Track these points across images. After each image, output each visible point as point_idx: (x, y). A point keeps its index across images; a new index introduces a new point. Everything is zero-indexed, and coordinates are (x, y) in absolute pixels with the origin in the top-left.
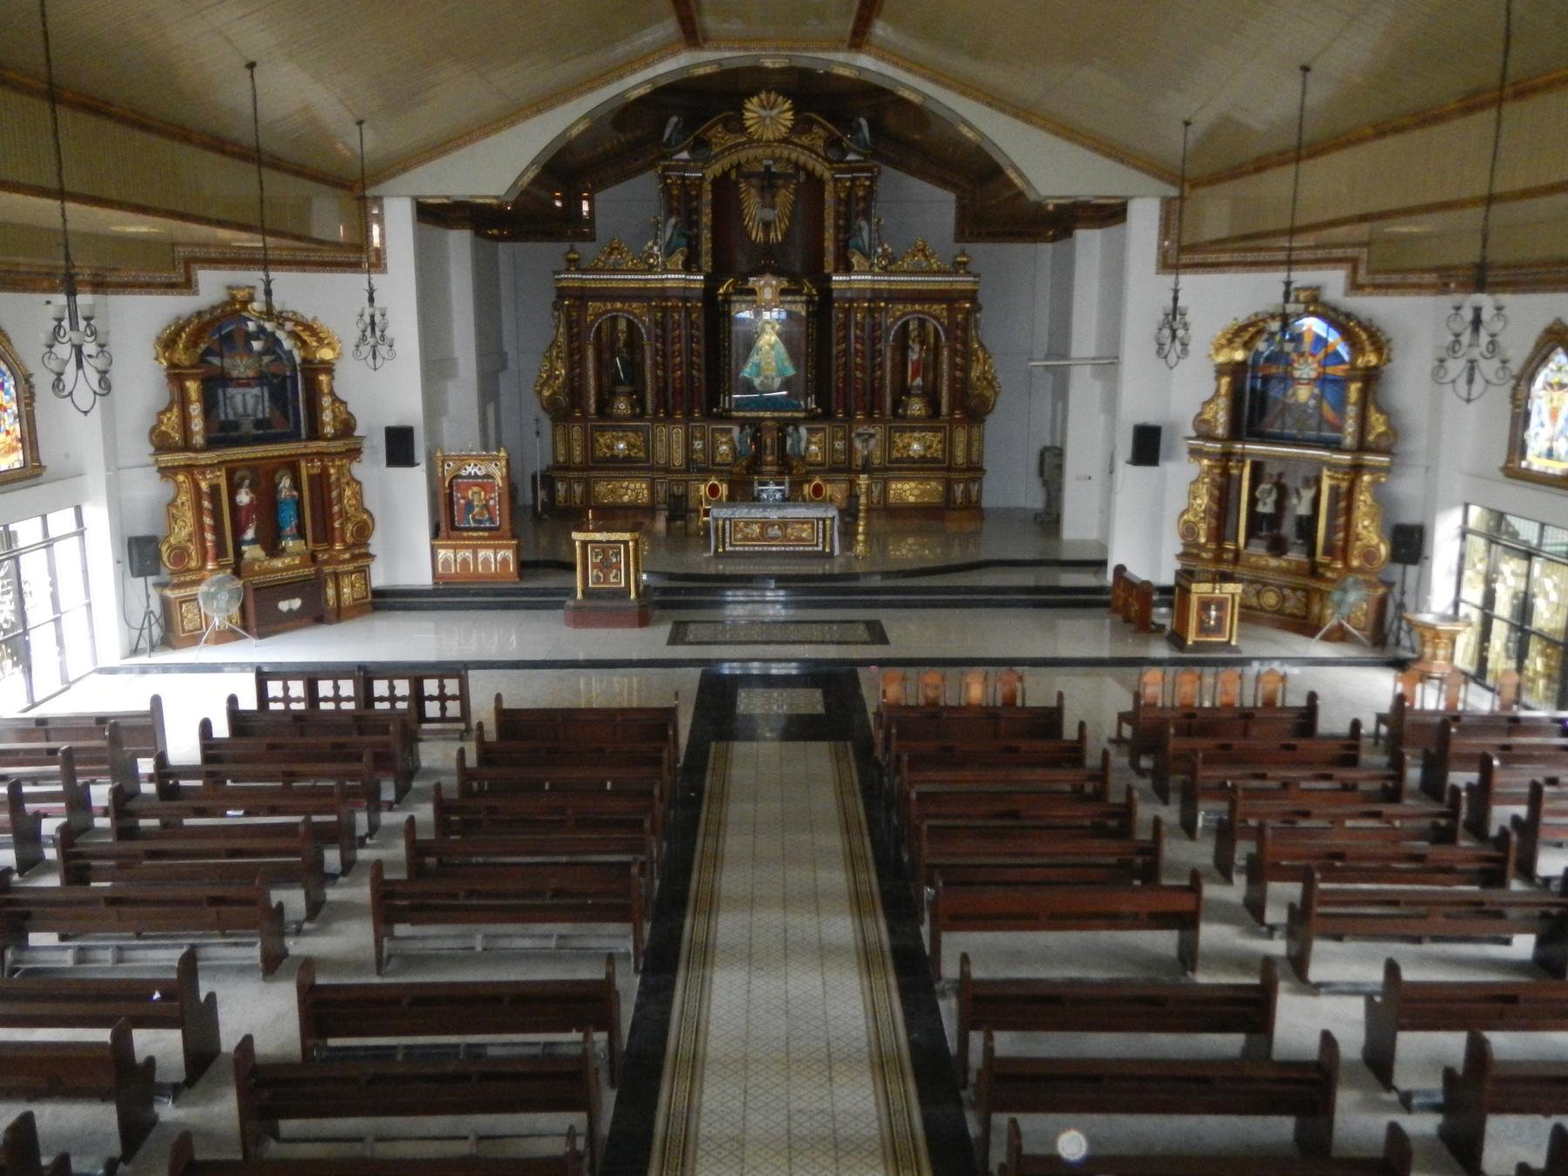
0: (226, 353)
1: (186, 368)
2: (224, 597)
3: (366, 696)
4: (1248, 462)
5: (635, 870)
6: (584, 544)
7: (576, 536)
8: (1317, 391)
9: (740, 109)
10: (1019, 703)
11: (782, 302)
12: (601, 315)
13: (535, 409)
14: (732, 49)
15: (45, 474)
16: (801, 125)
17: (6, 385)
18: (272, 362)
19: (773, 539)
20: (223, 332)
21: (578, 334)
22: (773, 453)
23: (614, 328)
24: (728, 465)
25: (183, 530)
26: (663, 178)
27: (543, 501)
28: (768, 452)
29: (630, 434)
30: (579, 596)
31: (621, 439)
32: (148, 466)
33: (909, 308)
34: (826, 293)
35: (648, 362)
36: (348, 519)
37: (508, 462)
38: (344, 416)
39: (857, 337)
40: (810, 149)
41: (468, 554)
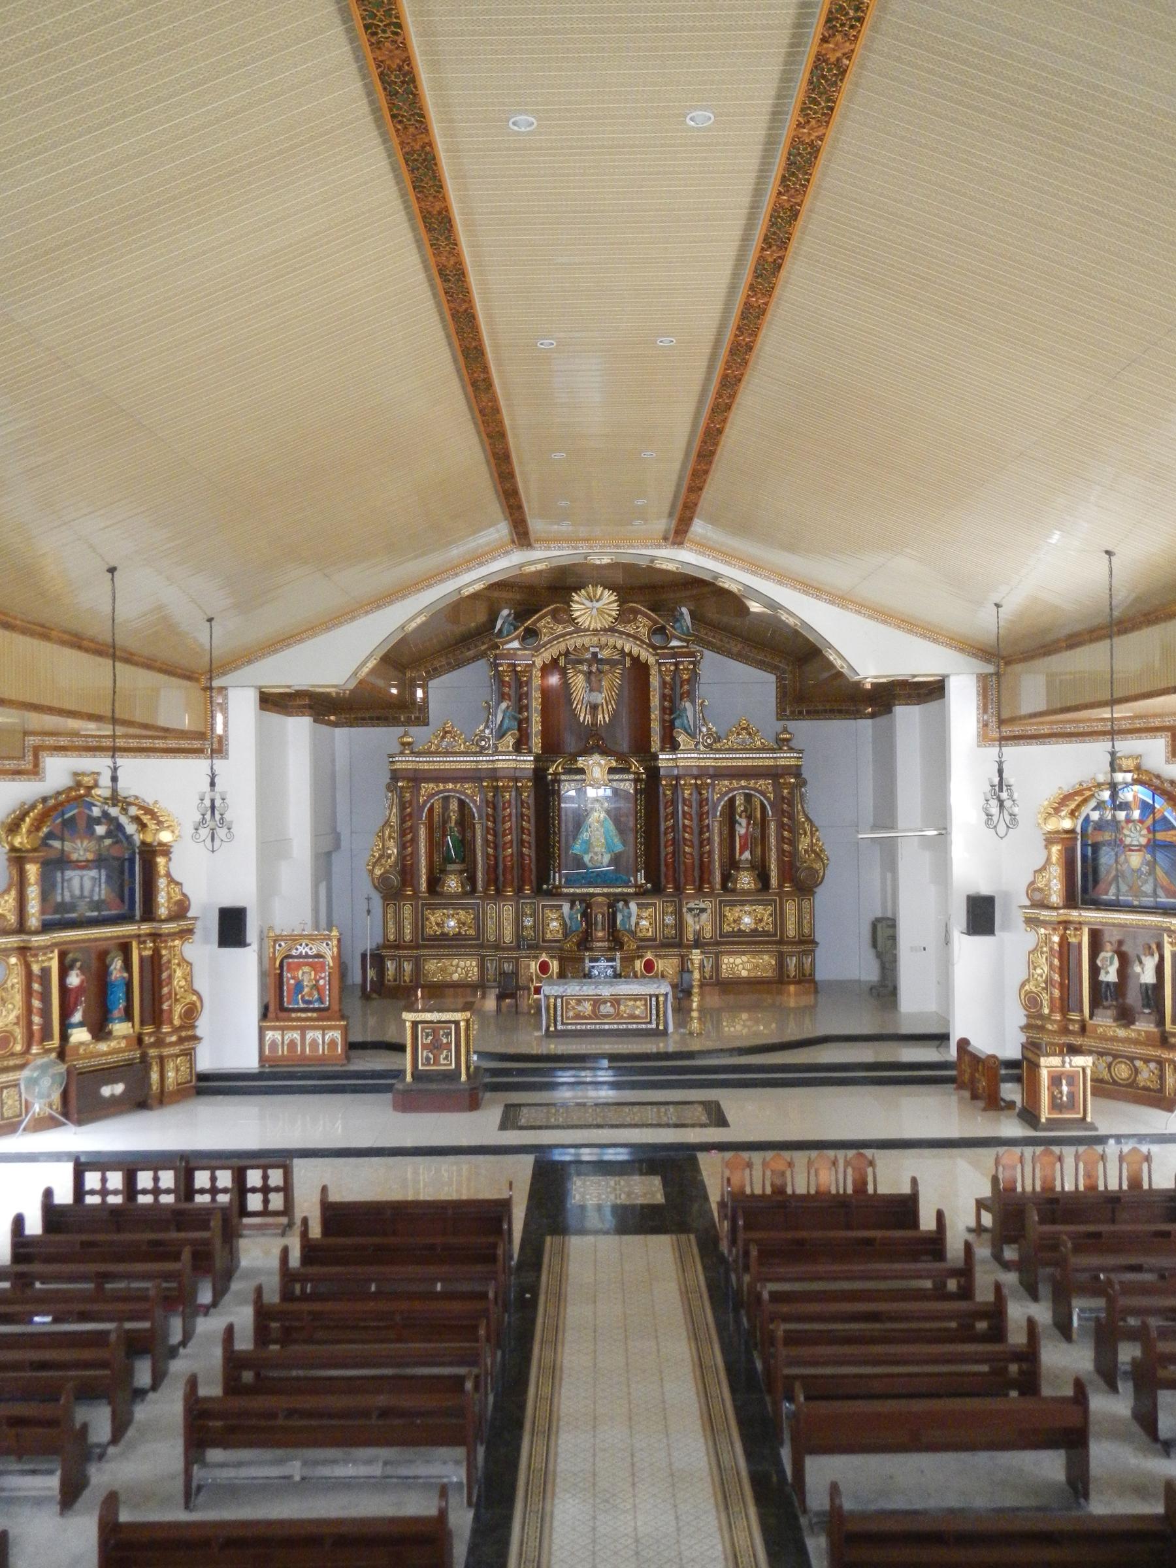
0: (67, 835)
1: (28, 851)
2: (46, 1082)
3: (186, 1189)
4: (1086, 931)
5: (469, 1385)
6: (415, 1024)
7: (409, 1016)
8: (1148, 857)
9: (568, 601)
10: (870, 1190)
11: (610, 781)
12: (433, 795)
13: (366, 887)
14: (560, 548)
16: (625, 615)
19: (605, 1016)
20: (66, 816)
21: (410, 815)
22: (603, 929)
23: (445, 808)
24: (556, 941)
26: (495, 666)
27: (372, 979)
28: (600, 927)
30: (409, 1078)
34: (653, 773)
35: (479, 841)
36: (177, 1000)
37: (339, 941)
38: (179, 897)
39: (684, 812)
40: (636, 638)
41: (296, 1035)
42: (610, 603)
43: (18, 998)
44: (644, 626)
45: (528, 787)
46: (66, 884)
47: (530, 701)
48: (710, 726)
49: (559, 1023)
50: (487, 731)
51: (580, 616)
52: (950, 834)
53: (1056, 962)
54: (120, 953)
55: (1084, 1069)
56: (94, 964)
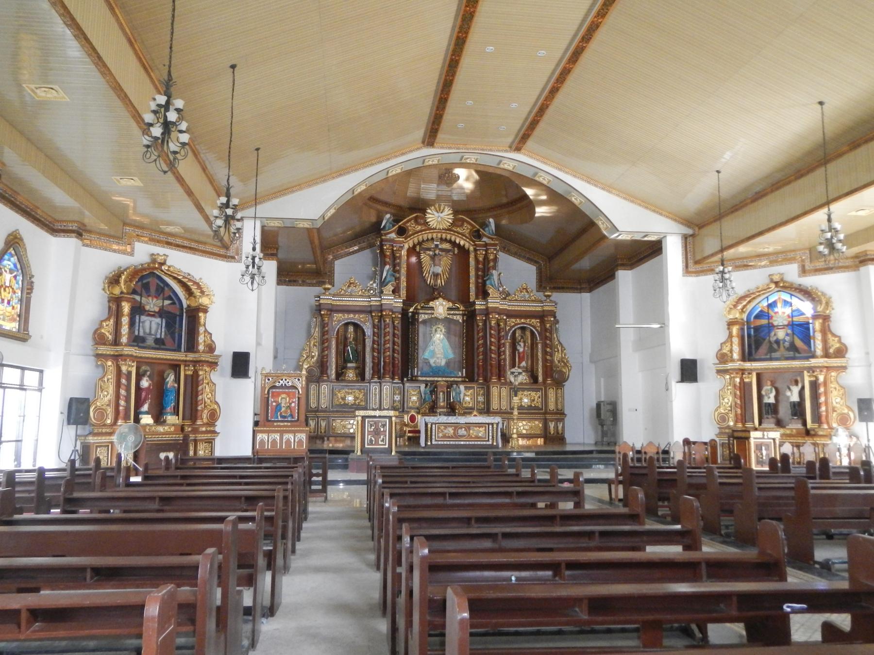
6: (364, 418)
8: (789, 331)
9: (424, 211)
14: (450, 148)
17: (18, 277)
18: (169, 304)
21: (327, 331)
25: (106, 397)
28: (441, 400)
29: (357, 391)
30: (359, 453)
32: (90, 355)
33: (518, 321)
41: (277, 436)
42: (448, 215)
43: (111, 389)
44: (468, 228)
45: (399, 318)
46: (141, 324)
47: (400, 268)
48: (505, 287)
49: (433, 440)
50: (375, 285)
51: (430, 221)
52: (668, 326)
53: (738, 393)
54: (173, 371)
55: (774, 439)
56: (156, 378)
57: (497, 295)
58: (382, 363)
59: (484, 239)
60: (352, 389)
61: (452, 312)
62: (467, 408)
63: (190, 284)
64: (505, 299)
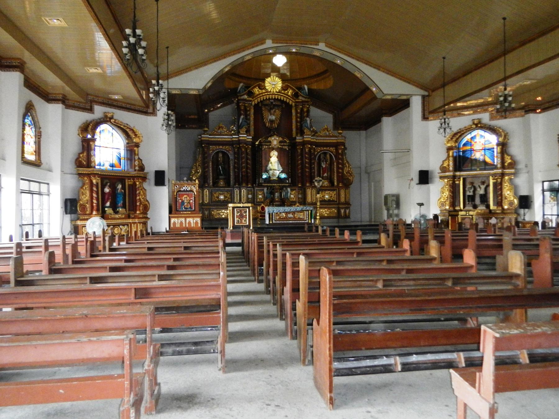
4: (462, 179)
9: (263, 81)
14: (281, 43)
15: (42, 166)
25: (85, 198)
29: (226, 193)
31: (222, 194)
35: (232, 167)
41: (183, 220)
47: (250, 117)
57: (309, 133)
58: (241, 176)
59: (300, 98)
60: (222, 192)
61: (282, 144)
62: (293, 202)
63: (128, 130)
64: (314, 135)
